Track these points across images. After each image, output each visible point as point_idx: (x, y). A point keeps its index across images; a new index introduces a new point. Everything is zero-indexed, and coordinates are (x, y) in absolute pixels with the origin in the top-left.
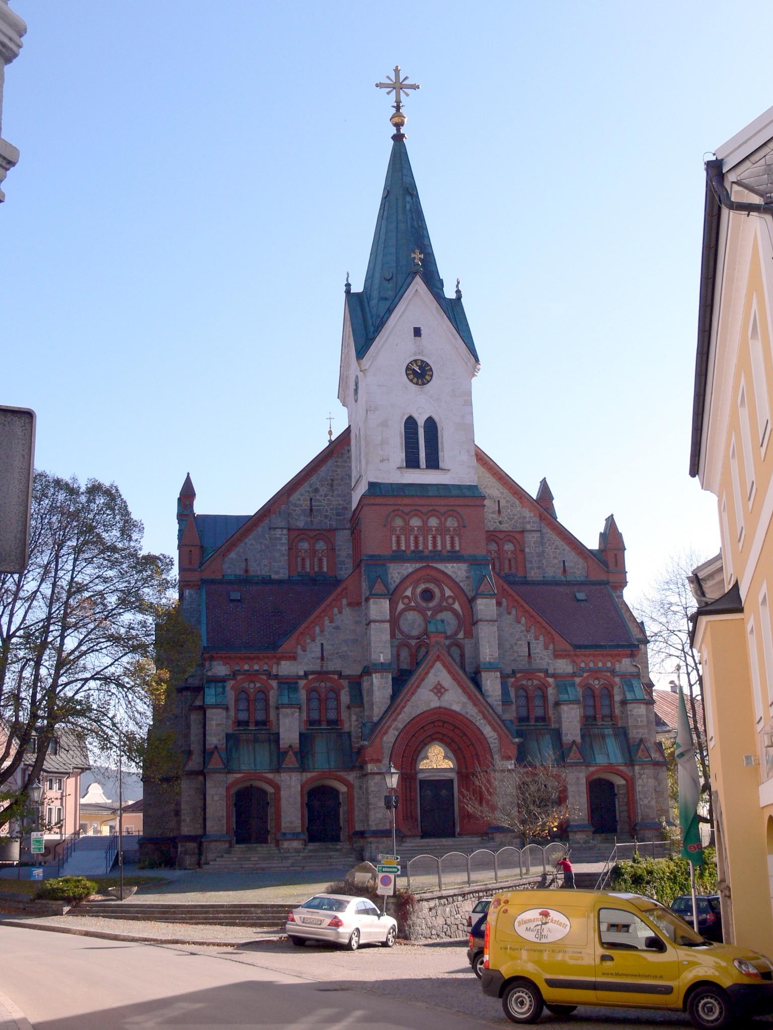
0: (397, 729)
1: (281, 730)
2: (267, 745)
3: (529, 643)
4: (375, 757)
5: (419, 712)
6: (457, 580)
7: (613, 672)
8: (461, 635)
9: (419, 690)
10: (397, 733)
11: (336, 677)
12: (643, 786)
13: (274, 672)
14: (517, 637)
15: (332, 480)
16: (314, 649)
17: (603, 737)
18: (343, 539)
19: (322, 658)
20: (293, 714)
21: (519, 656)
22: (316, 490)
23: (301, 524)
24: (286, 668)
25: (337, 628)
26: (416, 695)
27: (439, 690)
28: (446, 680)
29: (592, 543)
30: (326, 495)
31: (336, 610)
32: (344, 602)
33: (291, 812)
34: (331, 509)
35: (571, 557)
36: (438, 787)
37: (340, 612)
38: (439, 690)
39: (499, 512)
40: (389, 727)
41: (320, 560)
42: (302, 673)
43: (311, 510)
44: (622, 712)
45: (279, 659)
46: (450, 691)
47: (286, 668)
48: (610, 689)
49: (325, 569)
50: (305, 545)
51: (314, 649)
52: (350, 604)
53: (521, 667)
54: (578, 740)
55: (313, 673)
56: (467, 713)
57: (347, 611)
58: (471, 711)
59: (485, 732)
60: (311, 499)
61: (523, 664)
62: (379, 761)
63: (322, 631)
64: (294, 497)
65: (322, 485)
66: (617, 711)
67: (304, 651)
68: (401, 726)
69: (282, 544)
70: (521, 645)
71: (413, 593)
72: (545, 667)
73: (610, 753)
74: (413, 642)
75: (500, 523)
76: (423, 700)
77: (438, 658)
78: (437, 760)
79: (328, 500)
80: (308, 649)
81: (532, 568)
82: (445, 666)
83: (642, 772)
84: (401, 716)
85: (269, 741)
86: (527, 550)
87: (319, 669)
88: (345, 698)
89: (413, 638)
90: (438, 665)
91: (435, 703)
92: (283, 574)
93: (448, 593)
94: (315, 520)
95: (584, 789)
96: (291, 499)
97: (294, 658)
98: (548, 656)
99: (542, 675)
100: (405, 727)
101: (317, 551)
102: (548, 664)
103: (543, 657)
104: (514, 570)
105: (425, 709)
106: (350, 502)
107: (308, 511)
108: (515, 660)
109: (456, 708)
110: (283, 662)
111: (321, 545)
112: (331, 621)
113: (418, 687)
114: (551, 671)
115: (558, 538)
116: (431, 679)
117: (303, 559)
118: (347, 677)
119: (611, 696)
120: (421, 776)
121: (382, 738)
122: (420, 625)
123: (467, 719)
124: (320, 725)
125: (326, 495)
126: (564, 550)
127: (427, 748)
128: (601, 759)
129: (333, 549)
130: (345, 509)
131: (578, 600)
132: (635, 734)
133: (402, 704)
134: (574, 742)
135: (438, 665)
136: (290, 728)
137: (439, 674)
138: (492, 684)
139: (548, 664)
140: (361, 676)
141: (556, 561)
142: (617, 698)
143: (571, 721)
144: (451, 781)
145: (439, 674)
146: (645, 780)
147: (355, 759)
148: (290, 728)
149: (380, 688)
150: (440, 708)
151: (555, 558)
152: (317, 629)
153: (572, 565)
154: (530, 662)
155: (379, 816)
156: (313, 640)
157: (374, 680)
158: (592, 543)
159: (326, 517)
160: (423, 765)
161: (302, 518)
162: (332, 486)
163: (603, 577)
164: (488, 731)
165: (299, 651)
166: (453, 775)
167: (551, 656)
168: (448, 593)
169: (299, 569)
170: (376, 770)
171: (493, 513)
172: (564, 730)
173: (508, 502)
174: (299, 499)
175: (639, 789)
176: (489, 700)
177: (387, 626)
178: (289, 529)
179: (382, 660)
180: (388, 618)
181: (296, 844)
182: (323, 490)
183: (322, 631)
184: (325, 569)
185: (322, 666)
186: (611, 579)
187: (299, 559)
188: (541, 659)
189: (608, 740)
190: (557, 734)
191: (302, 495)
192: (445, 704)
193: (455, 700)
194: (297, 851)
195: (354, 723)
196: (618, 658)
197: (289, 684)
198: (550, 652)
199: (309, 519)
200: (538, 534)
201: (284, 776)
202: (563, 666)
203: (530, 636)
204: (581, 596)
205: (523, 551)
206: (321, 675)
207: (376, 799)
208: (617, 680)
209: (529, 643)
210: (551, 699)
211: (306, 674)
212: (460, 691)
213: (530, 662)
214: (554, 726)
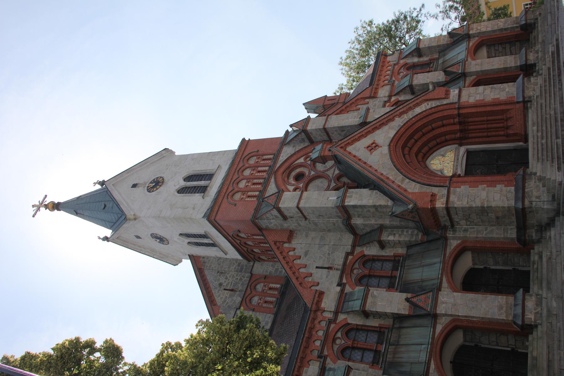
0: (403, 181)
1: (388, 310)
2: (404, 331)
6: (293, 152)
9: (368, 163)
10: (407, 180)
13: (329, 315)
15: (218, 272)
16: (319, 276)
18: (260, 269)
19: (329, 268)
20: (374, 297)
22: (221, 285)
23: (239, 299)
24: (329, 303)
25: (306, 254)
30: (226, 278)
33: (488, 307)
34: (237, 275)
37: (294, 249)
41: (270, 289)
42: (339, 289)
43: (232, 290)
45: (318, 309)
47: (329, 303)
49: (278, 286)
50: (256, 300)
52: (289, 241)
55: (341, 278)
57: (295, 243)
58: (399, 122)
60: (225, 289)
63: (305, 266)
64: (219, 301)
65: (219, 280)
67: (318, 284)
71: (293, 185)
74: (333, 184)
79: (230, 277)
80: (317, 280)
85: (400, 328)
87: (339, 272)
88: (372, 250)
91: (385, 150)
93: (302, 160)
94: (240, 288)
96: (219, 304)
97: (321, 294)
100: (401, 173)
101: (263, 290)
105: (388, 157)
106: (237, 260)
107: (232, 293)
109: (392, 133)
111: (260, 287)
112: (300, 258)
114: (386, 99)
117: (266, 302)
118: (354, 246)
121: (409, 193)
122: (322, 182)
124: (395, 277)
125: (226, 278)
129: (265, 277)
130: (239, 264)
137: (358, 149)
139: (380, 101)
140: (352, 229)
144: (469, 153)
147: (431, 225)
148: (388, 302)
149: (359, 198)
150: (389, 145)
152: (302, 270)
155: (497, 196)
156: (311, 275)
157: (352, 203)
159: (241, 279)
161: (234, 298)
162: (222, 273)
165: (317, 288)
168: (302, 160)
169: (272, 306)
174: (221, 298)
181: (530, 304)
182: (222, 280)
183: (305, 266)
184: (278, 286)
185: (337, 269)
187: (265, 305)
191: (219, 296)
192: (388, 142)
193: (384, 136)
194: (539, 303)
195: (397, 238)
197: (343, 299)
199: (238, 293)
201: (441, 310)
208: (402, 62)
212: (378, 132)
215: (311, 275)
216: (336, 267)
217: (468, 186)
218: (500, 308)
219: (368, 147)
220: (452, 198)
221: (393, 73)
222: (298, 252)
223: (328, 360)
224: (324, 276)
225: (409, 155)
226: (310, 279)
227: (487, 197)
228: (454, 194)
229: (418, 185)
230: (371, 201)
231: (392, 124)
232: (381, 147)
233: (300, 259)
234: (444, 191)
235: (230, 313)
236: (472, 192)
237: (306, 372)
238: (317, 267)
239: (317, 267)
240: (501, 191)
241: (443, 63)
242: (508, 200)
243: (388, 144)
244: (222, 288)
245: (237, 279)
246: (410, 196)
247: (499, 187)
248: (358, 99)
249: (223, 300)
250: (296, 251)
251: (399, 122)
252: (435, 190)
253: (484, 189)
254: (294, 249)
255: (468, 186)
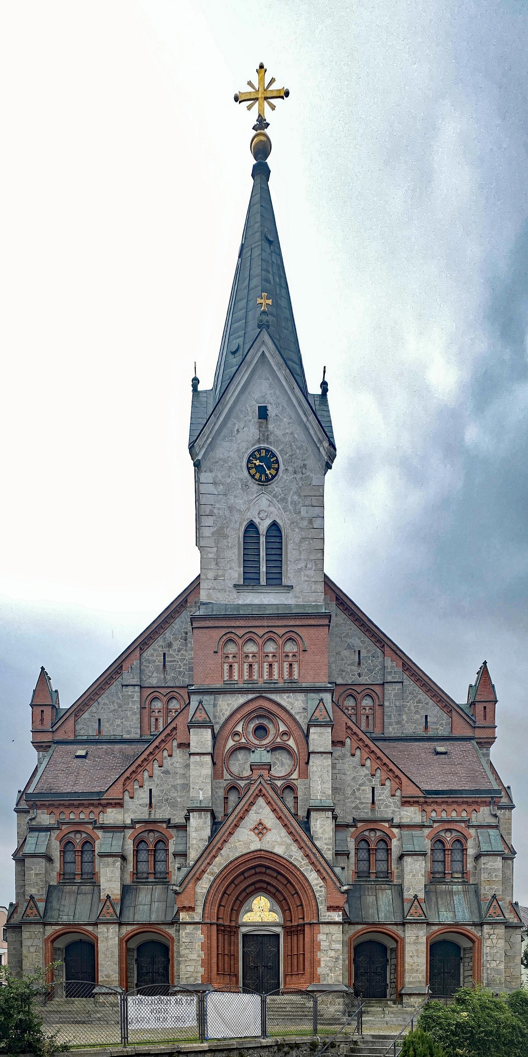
0: (212, 874)
3: (373, 788)
4: (186, 904)
5: (237, 855)
7: (467, 822)
8: (295, 776)
10: (212, 878)
11: (164, 825)
12: (491, 947)
14: (360, 782)
16: (142, 796)
17: (451, 893)
21: (362, 803)
22: (170, 645)
25: (167, 772)
26: (236, 834)
27: (262, 833)
28: (269, 819)
29: (461, 697)
31: (166, 753)
32: (175, 743)
34: (185, 665)
35: (435, 712)
36: (261, 942)
38: (260, 829)
39: (359, 664)
40: (203, 872)
44: (475, 868)
46: (273, 831)
48: (463, 841)
51: (142, 796)
53: (363, 816)
54: (421, 895)
56: (291, 856)
58: (296, 856)
59: (310, 879)
60: (164, 654)
61: (366, 813)
62: (192, 909)
63: (151, 777)
66: (470, 865)
67: (132, 798)
68: (217, 871)
69: (133, 702)
70: (363, 790)
72: (390, 816)
73: (455, 910)
75: (359, 675)
76: (244, 842)
77: (260, 794)
78: (261, 912)
79: (182, 655)
81: (390, 724)
82: (269, 803)
83: (492, 932)
84: (217, 859)
86: (386, 704)
89: (242, 779)
90: (261, 801)
91: (255, 845)
92: (135, 734)
95: (423, 948)
97: (119, 804)
98: (395, 803)
99: (386, 825)
100: (222, 871)
102: (394, 812)
103: (390, 807)
104: (371, 726)
105: (245, 851)
107: (161, 667)
108: (356, 808)
109: (279, 850)
110: (109, 810)
113: (236, 826)
115: (421, 691)
116: (252, 818)
119: (464, 850)
120: (244, 930)
123: (291, 863)
126: (427, 704)
127: (251, 899)
128: (446, 917)
131: (438, 753)
132: (486, 891)
133: (219, 845)
134: (416, 897)
135: (261, 801)
136: (110, 879)
137: (262, 812)
138: (322, 827)
141: (418, 716)
142: (471, 851)
143: (414, 875)
145: (262, 812)
146: (495, 941)
149: (200, 829)
150: (261, 850)
151: (417, 712)
153: (435, 720)
154: (373, 810)
155: (191, 969)
158: (461, 697)
159: (180, 672)
160: (247, 918)
162: (186, 640)
163: (468, 732)
164: (313, 877)
166: (279, 930)
167: (399, 803)
170: (188, 920)
171: (352, 664)
172: (406, 885)
173: (368, 651)
174: (152, 655)
175: (486, 950)
176: (318, 843)
177: (208, 759)
178: (141, 687)
179: (201, 798)
180: (210, 750)
182: (176, 645)
186: (478, 733)
188: (387, 806)
189: (455, 898)
190: (400, 889)
193: (278, 842)
196: (475, 807)
198: (397, 799)
200: (399, 686)
202: (411, 815)
203: (375, 782)
204: (440, 749)
205: (382, 705)
206: (150, 824)
207: (187, 951)
209: (373, 788)
210: (395, 853)
211: (134, 822)
213: (373, 810)
214: (396, 881)
215: (141, 787)
216: (153, 812)
217: (203, 941)
218: (108, 976)
219: (260, 823)
220: (189, 928)
221: (449, 822)
222: (167, 763)
223: (57, 832)
224: (141, 802)
225: (256, 873)
226: (136, 787)
227: (190, 960)
228: (193, 929)
229: (205, 891)
230: (194, 842)
231: (294, 848)
232: (260, 840)
233: (159, 767)
234: (197, 920)
235: (133, 678)
236: (197, 945)
237: (43, 813)
238: (151, 790)
239: (151, 790)
240: (197, 972)
241: (451, 893)
242: (186, 978)
243: (262, 848)
244: (166, 650)
245: (180, 668)
246: (190, 885)
247: (202, 970)
248: (400, 779)
249: (151, 658)
250: (169, 758)
251: (296, 856)
252: (199, 910)
253: (199, 956)
254: (170, 756)
255: (203, 941)
